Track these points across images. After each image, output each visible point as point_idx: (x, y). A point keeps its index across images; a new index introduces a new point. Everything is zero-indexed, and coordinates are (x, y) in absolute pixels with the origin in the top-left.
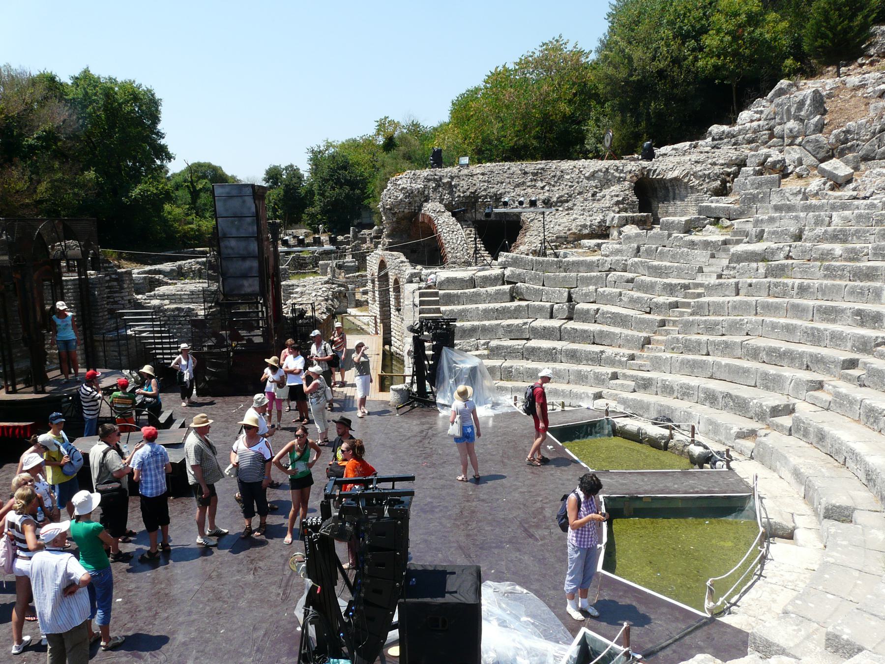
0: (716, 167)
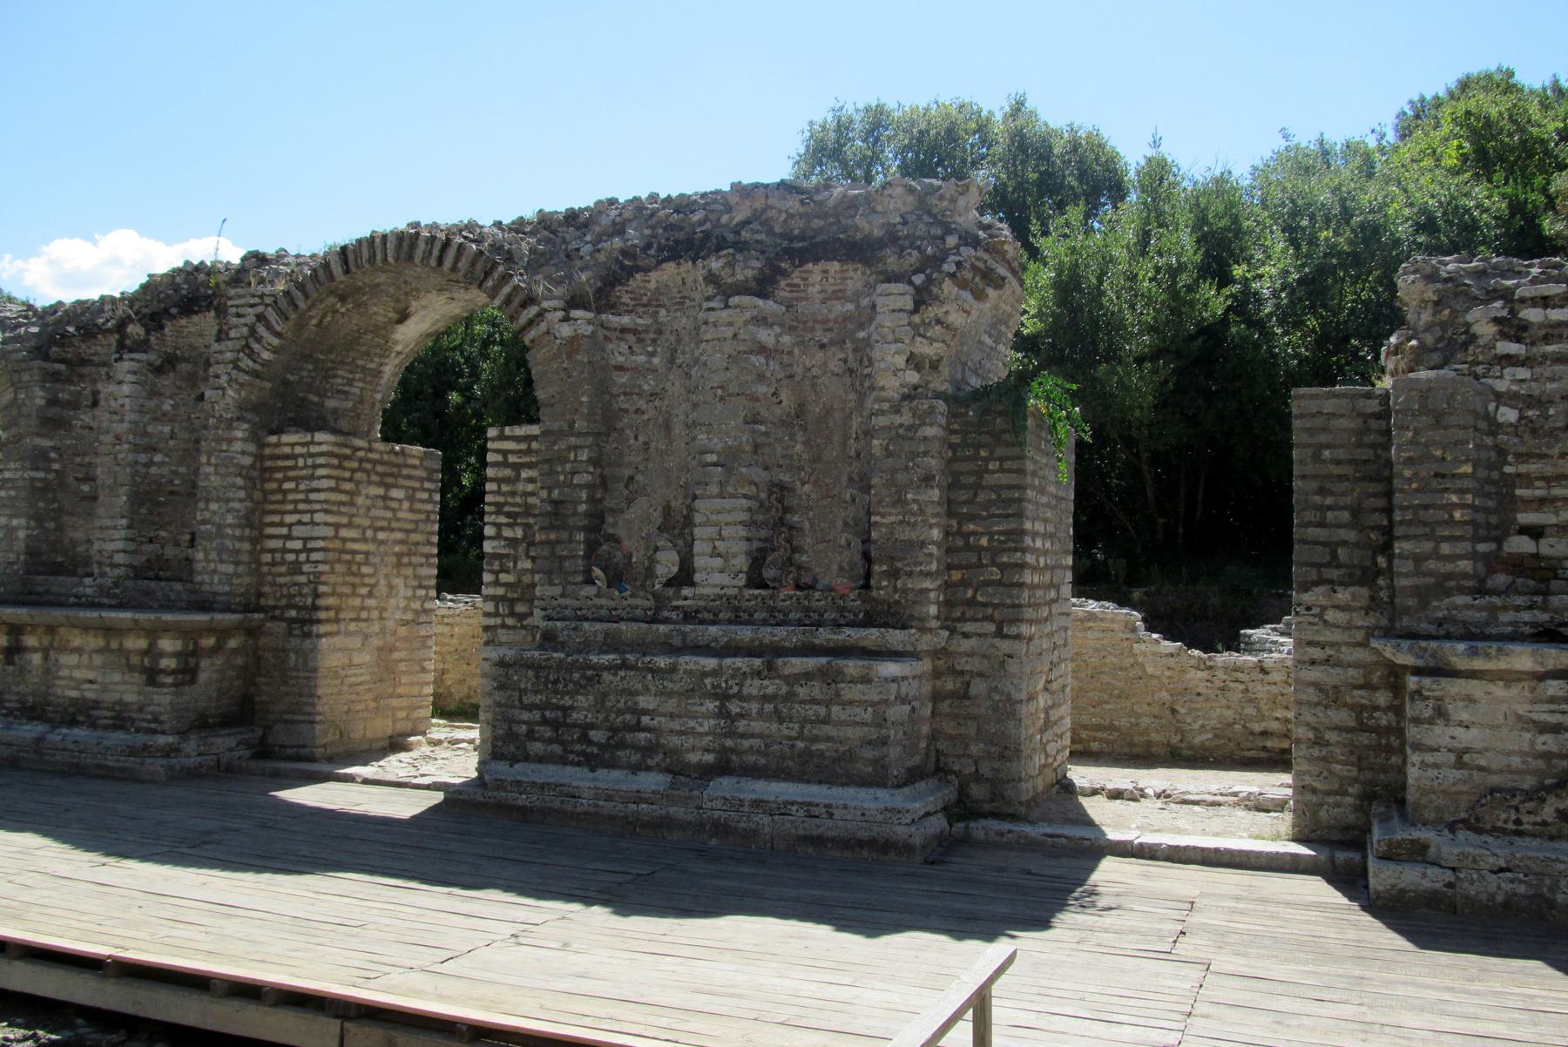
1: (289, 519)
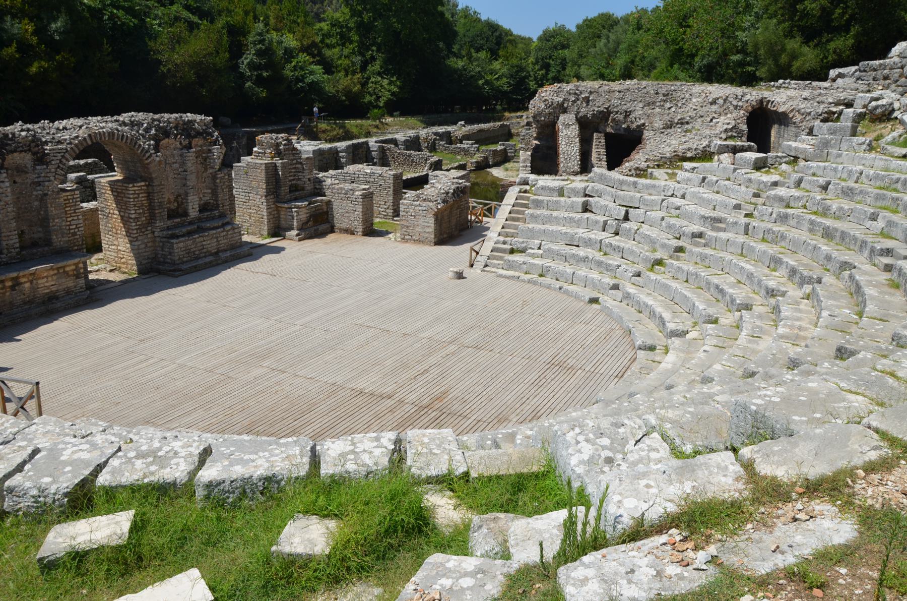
0: (822, 106)
1: (69, 219)
